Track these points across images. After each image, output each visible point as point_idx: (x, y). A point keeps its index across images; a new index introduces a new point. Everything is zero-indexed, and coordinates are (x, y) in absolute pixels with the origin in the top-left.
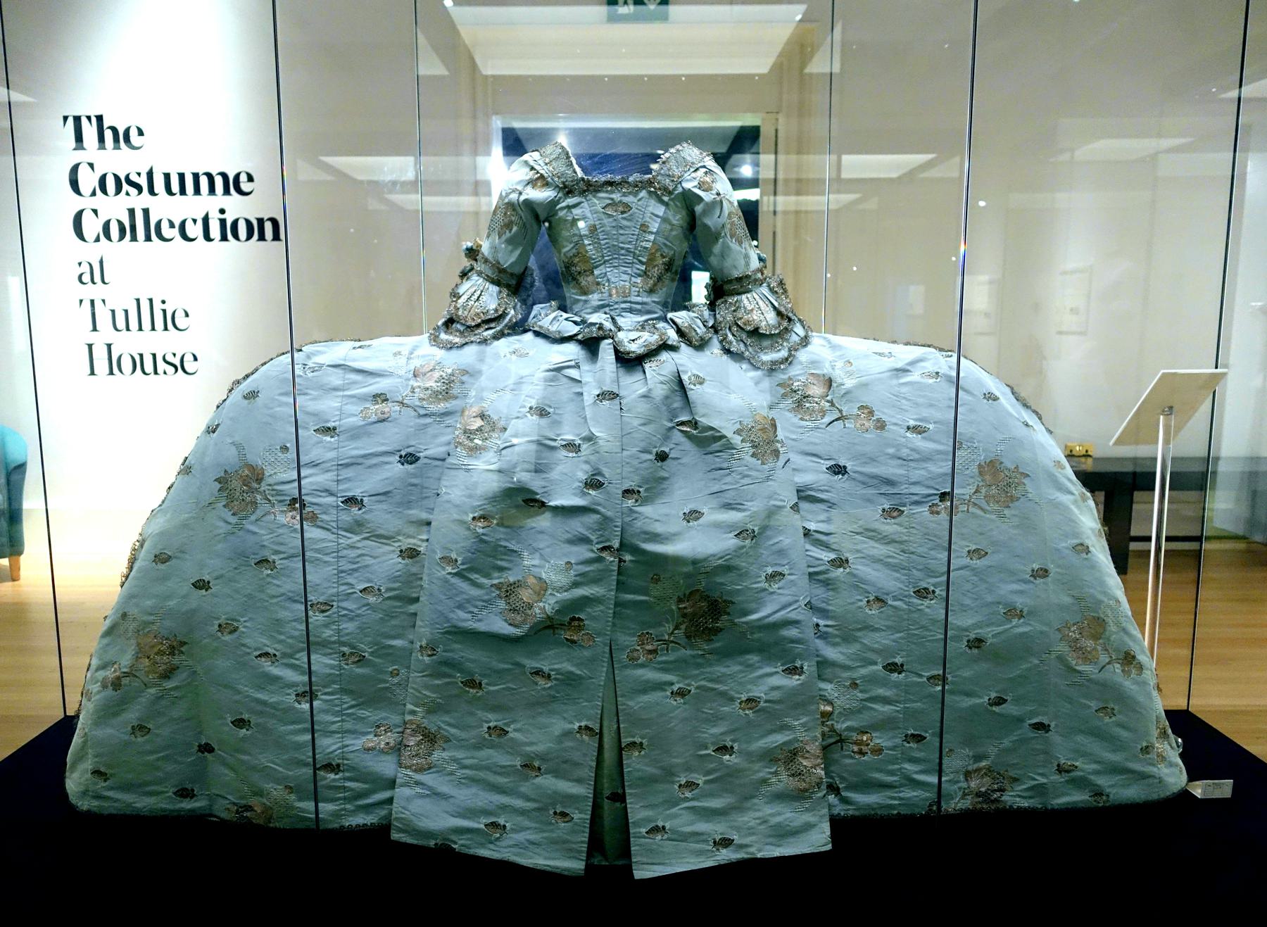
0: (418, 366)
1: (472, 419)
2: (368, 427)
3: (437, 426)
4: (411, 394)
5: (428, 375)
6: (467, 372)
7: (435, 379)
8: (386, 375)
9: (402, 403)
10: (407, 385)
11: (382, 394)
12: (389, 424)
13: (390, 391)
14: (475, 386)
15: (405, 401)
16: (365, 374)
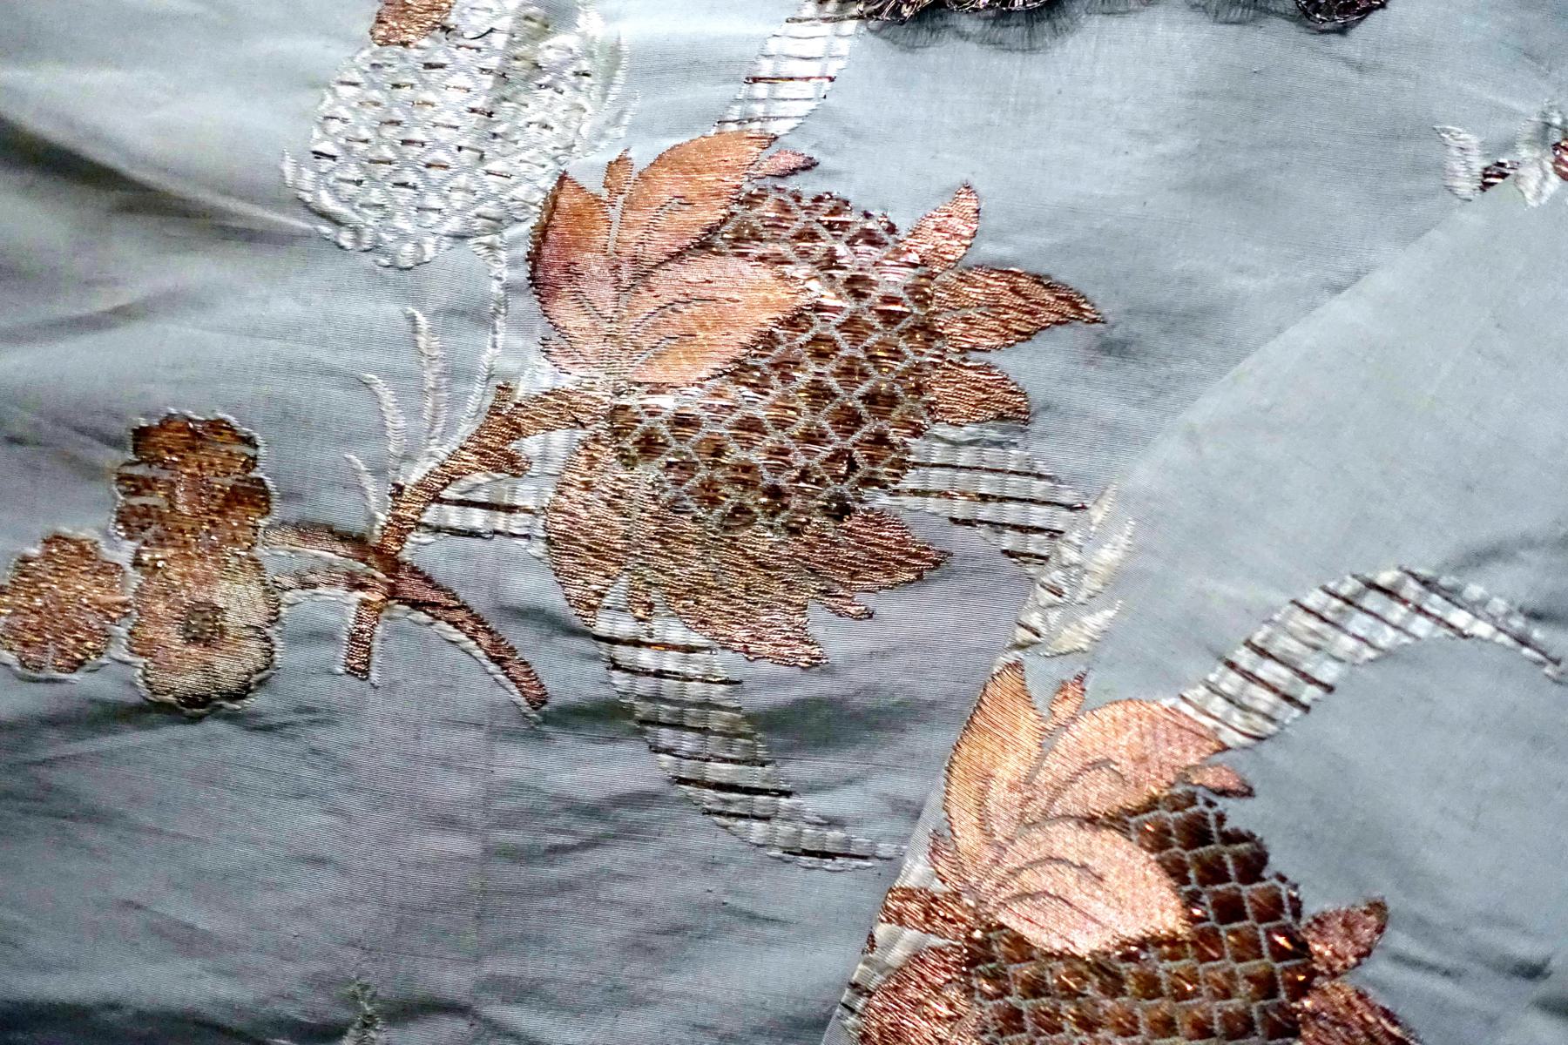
0: (588, 169)
1: (1068, 840)
2: (55, 745)
3: (703, 838)
4: (481, 482)
5: (669, 282)
6: (1074, 307)
7: (734, 341)
8: (253, 236)
9: (393, 565)
10: (457, 373)
11: (217, 426)
12: (254, 747)
13: (287, 417)
14: (1143, 474)
15: (419, 549)
16: (115, 196)
